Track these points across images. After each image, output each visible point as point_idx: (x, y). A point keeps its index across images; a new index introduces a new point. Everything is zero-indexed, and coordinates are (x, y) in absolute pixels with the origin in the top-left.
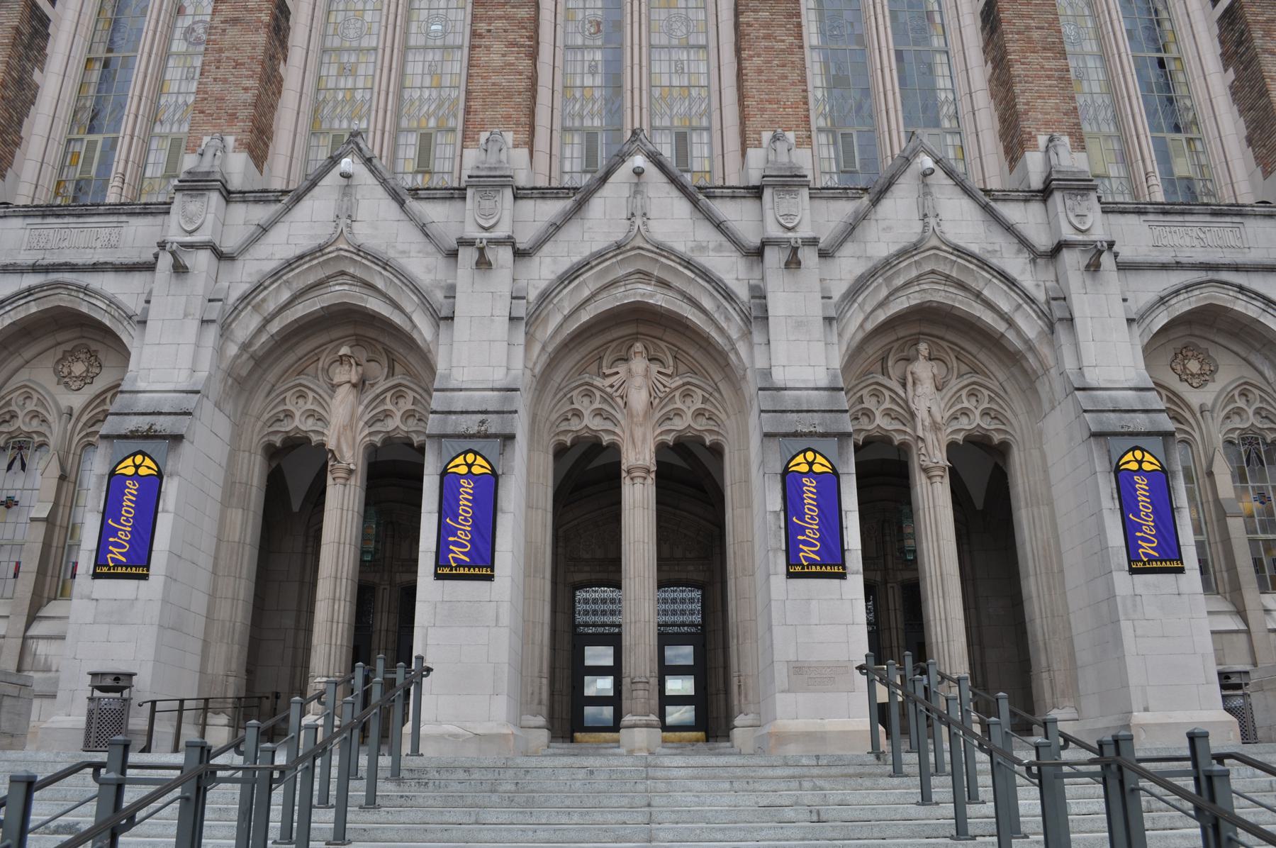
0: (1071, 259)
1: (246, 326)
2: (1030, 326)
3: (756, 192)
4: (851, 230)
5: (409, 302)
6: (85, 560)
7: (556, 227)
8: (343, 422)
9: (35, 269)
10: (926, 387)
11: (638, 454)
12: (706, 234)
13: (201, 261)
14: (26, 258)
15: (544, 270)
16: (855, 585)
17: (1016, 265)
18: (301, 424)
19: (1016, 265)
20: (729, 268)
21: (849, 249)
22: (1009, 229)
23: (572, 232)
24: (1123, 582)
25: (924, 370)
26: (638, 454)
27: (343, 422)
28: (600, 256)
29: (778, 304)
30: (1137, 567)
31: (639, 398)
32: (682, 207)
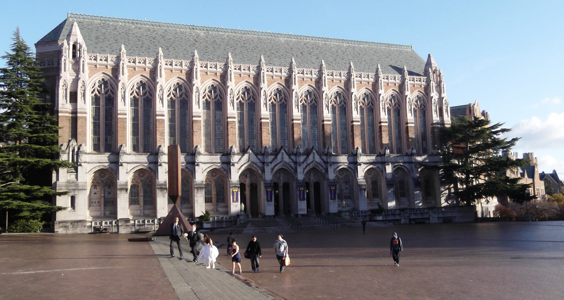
2: (324, 171)
5: (258, 169)
6: (231, 201)
7: (273, 160)
9: (212, 163)
10: (312, 177)
12: (291, 161)
14: (210, 161)
16: (306, 201)
17: (323, 164)
19: (323, 164)
20: (292, 164)
21: (305, 162)
22: (323, 159)
23: (276, 160)
24: (330, 201)
26: (281, 184)
28: (279, 163)
30: (331, 199)
31: (281, 178)
32: (287, 157)
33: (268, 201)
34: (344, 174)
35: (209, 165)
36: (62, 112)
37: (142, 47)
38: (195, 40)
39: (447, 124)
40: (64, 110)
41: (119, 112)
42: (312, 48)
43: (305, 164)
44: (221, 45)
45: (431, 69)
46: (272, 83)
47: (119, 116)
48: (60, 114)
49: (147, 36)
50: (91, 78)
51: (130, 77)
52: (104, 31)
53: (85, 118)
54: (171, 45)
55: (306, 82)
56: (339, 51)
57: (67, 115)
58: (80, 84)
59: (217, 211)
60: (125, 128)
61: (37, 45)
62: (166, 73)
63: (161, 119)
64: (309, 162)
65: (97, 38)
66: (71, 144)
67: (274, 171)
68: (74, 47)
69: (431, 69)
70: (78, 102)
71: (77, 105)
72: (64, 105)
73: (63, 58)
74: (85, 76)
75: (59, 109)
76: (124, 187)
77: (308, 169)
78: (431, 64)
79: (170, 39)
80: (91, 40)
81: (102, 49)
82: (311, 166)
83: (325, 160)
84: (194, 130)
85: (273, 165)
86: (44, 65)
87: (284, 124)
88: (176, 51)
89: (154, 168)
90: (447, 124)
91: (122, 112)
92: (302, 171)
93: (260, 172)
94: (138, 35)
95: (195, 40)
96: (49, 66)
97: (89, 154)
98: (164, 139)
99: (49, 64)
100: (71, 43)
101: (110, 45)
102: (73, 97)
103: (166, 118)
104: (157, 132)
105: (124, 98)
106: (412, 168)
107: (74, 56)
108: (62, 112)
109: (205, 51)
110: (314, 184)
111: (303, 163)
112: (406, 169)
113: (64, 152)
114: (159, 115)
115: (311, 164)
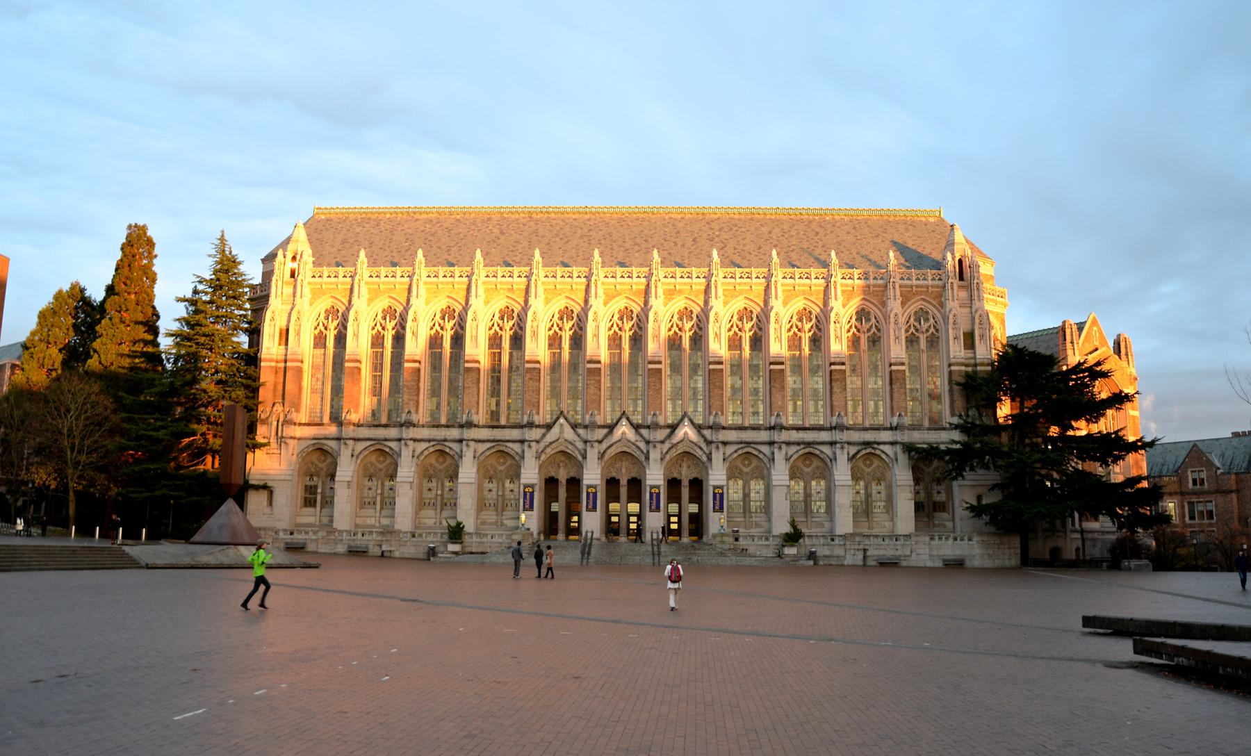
0: (714, 445)
1: (543, 457)
2: (704, 458)
3: (648, 427)
4: (669, 436)
7: (606, 436)
8: (563, 475)
9: (494, 441)
11: (624, 482)
12: (639, 438)
13: (533, 444)
15: (604, 445)
17: (703, 445)
18: (553, 474)
22: (703, 436)
25: (685, 465)
26: (624, 482)
27: (563, 475)
29: (652, 456)
33: (588, 510)
34: (753, 465)
35: (488, 445)
36: (266, 360)
38: (502, 233)
39: (982, 364)
42: (720, 230)
43: (667, 446)
44: (543, 237)
45: (953, 254)
46: (614, 297)
47: (347, 364)
51: (370, 301)
52: (358, 230)
55: (680, 292)
56: (776, 231)
57: (273, 364)
59: (502, 524)
62: (428, 290)
64: (675, 441)
65: (344, 242)
67: (607, 457)
69: (953, 254)
72: (270, 347)
73: (274, 279)
74: (303, 303)
77: (673, 453)
78: (953, 244)
82: (681, 449)
83: (709, 438)
85: (604, 445)
87: (637, 371)
89: (397, 449)
90: (982, 364)
92: (659, 457)
93: (580, 458)
95: (502, 233)
97: (300, 424)
106: (896, 454)
108: (266, 360)
110: (690, 481)
111: (663, 442)
112: (884, 456)
115: (680, 445)
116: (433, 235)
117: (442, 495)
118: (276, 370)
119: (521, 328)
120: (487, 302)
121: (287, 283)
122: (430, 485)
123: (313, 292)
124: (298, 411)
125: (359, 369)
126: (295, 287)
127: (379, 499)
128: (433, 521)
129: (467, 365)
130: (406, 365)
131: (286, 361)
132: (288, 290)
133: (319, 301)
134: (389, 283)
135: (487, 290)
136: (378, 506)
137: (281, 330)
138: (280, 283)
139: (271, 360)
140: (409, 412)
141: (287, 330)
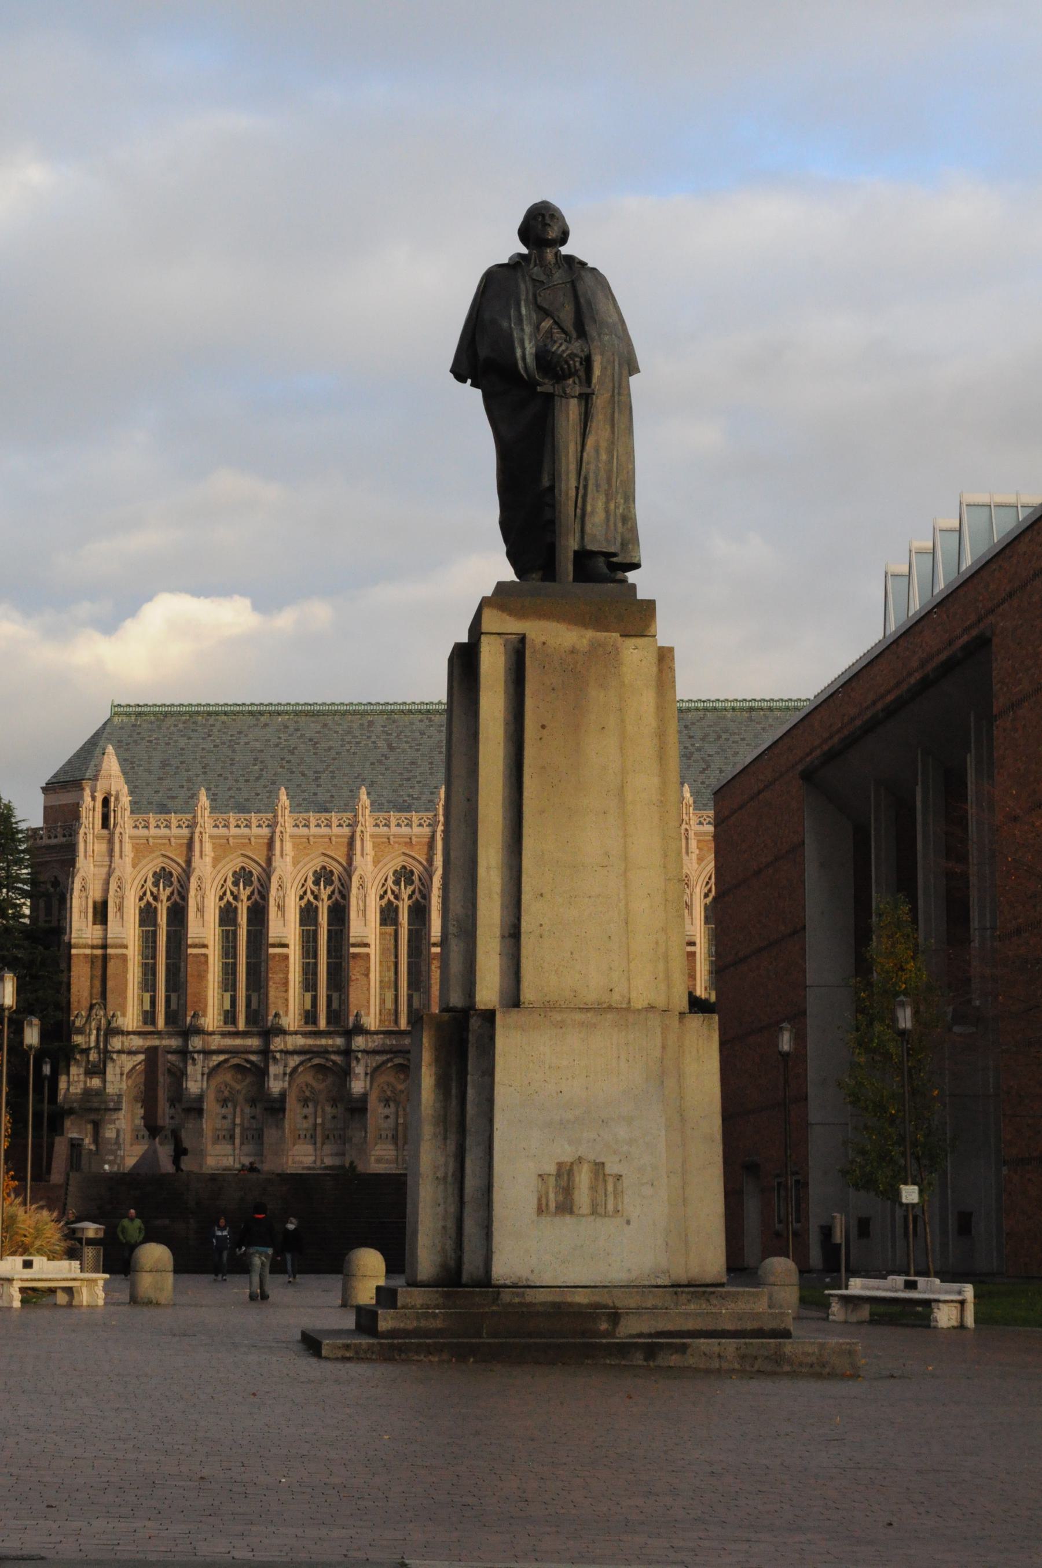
36: (77, 947)
37: (258, 779)
38: (391, 748)
40: (81, 941)
41: (190, 941)
48: (74, 951)
49: (277, 745)
50: (138, 868)
51: (216, 861)
53: (124, 958)
54: (328, 766)
57: (88, 951)
58: (113, 886)
60: (202, 976)
61: (45, 790)
62: (295, 846)
63: (279, 955)
65: (165, 764)
66: (94, 1011)
68: (106, 802)
70: (109, 923)
71: (106, 930)
72: (82, 930)
73: (82, 831)
75: (73, 941)
76: (195, 1105)
79: (330, 749)
80: (150, 772)
81: (170, 793)
84: (353, 977)
86: (56, 837)
88: (336, 782)
91: (197, 941)
94: (258, 745)
96: (64, 839)
98: (287, 1000)
99: (64, 836)
100: (100, 797)
101: (189, 780)
102: (101, 913)
103: (294, 954)
104: (271, 983)
105: (201, 910)
107: (105, 824)
109: (406, 775)
113: (80, 1031)
114: (274, 946)
116: (293, 754)
117: (323, 1124)
118: (93, 959)
119: (424, 897)
120: (376, 862)
121: (99, 838)
122: (306, 1111)
123: (136, 848)
124: (124, 1015)
125: (206, 956)
126: (111, 841)
127: (238, 1130)
128: (312, 1158)
129: (352, 950)
130: (271, 951)
131: (104, 947)
132: (101, 847)
133: (144, 862)
134: (242, 836)
135: (375, 846)
136: (237, 1141)
137: (95, 903)
138: (90, 837)
139: (85, 946)
140: (277, 1015)
141: (105, 904)
